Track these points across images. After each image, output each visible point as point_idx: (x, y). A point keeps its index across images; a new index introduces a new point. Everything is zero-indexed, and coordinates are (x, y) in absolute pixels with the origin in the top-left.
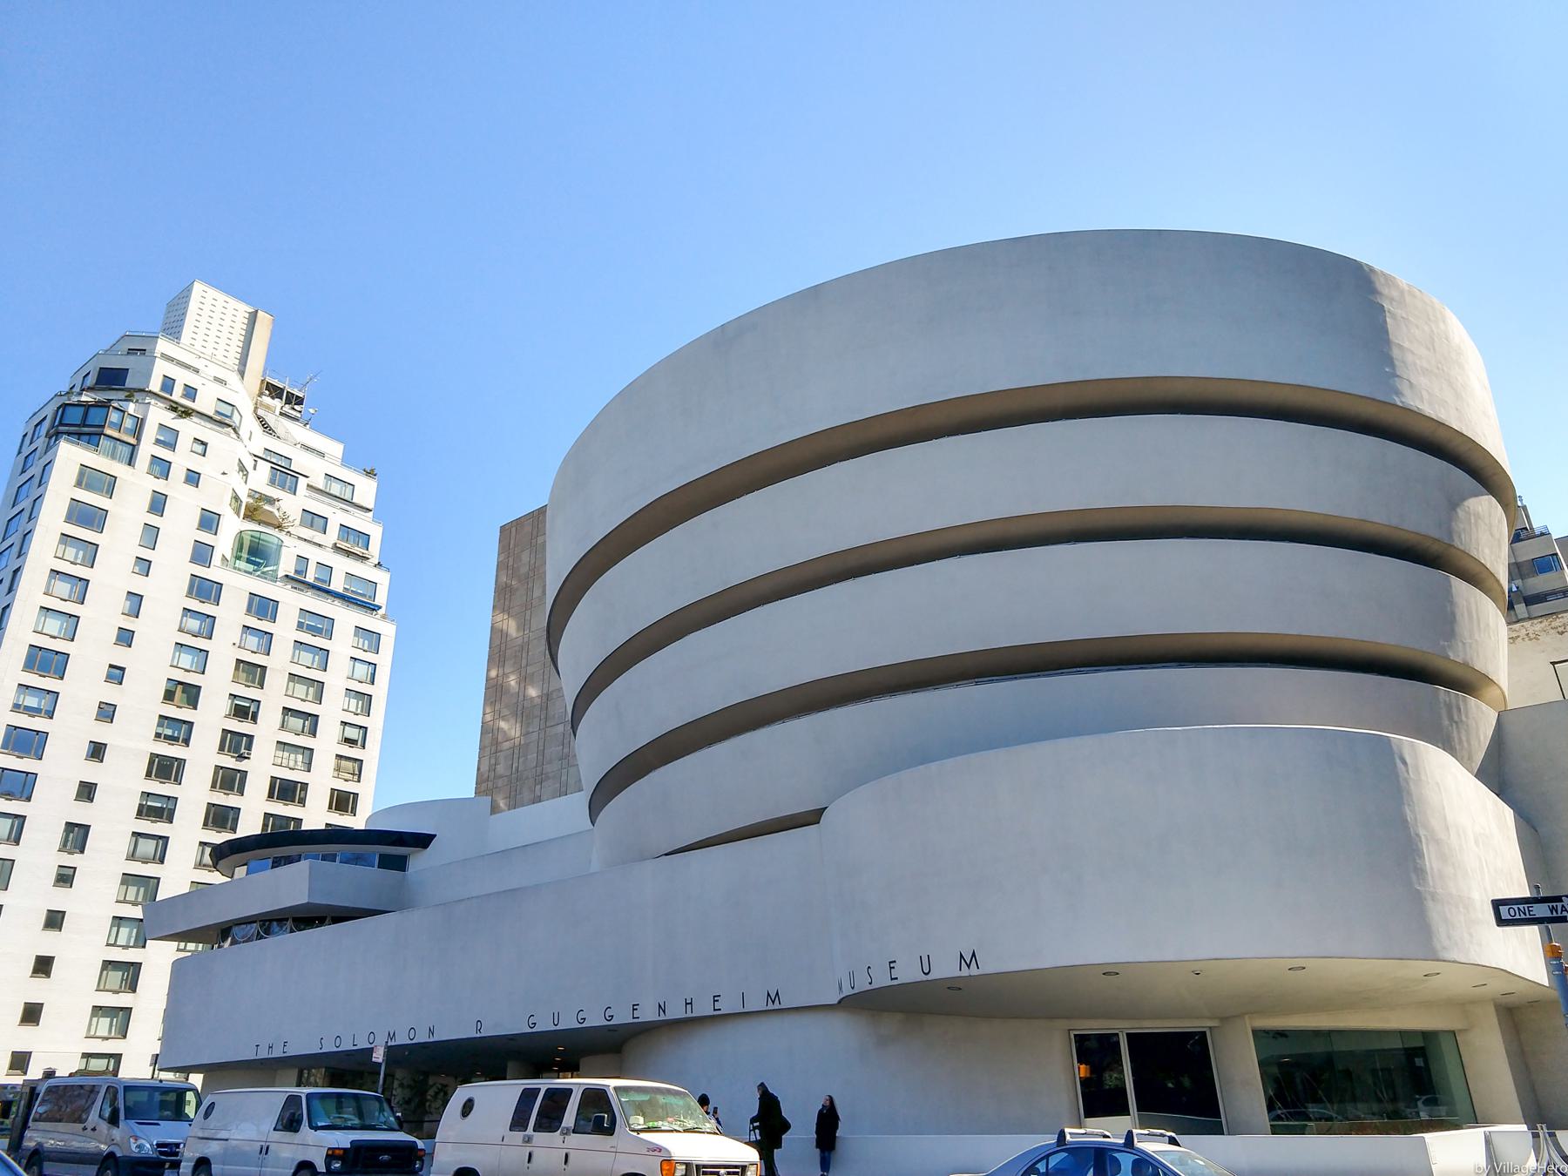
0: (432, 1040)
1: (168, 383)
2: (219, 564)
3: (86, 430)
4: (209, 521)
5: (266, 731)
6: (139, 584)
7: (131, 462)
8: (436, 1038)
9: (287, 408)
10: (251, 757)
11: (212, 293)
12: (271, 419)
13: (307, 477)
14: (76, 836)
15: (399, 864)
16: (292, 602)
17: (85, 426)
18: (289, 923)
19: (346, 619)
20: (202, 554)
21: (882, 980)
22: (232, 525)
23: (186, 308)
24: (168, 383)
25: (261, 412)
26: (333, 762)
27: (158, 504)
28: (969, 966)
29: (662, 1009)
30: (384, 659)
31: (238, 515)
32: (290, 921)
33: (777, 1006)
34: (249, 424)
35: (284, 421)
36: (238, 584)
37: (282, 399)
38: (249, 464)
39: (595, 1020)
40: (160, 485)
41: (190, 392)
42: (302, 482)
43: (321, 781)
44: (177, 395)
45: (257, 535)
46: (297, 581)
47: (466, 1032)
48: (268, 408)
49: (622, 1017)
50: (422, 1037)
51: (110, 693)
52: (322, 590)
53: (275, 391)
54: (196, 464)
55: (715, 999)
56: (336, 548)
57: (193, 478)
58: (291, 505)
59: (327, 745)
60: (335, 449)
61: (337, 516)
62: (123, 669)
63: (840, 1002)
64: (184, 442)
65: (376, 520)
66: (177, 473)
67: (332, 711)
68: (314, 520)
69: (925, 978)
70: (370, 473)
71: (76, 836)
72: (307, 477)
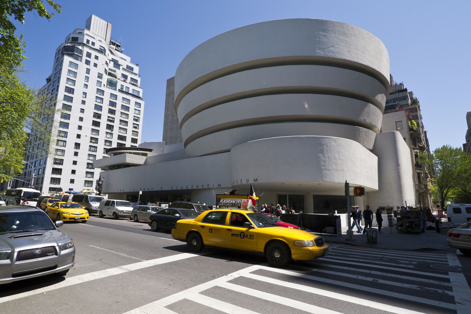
0: (152, 190)
1: (88, 41)
2: (103, 86)
4: (100, 76)
5: (116, 124)
6: (85, 90)
7: (81, 61)
8: (154, 190)
9: (117, 48)
10: (114, 130)
11: (97, 18)
12: (113, 51)
13: (122, 66)
14: (77, 145)
15: (146, 155)
16: (120, 95)
18: (123, 166)
19: (133, 100)
20: (99, 83)
21: (239, 183)
22: (106, 78)
23: (91, 22)
24: (88, 41)
26: (131, 132)
27: (88, 71)
28: (256, 181)
29: (198, 186)
30: (142, 109)
31: (107, 74)
32: (123, 166)
33: (220, 187)
34: (108, 52)
35: (116, 51)
36: (108, 91)
37: (115, 46)
38: (108, 62)
39: (184, 188)
40: (88, 67)
41: (93, 44)
42: (121, 67)
43: (129, 136)
44: (90, 44)
45: (111, 79)
46: (121, 91)
47: (160, 189)
48: (112, 48)
49: (190, 188)
50: (150, 190)
52: (127, 93)
53: (114, 44)
54: (96, 61)
55: (208, 185)
56: (130, 83)
57: (95, 65)
58: (119, 73)
59: (130, 128)
60: (128, 59)
61: (130, 76)
62: (84, 110)
63: (232, 187)
64: (93, 56)
65: (139, 76)
66: (92, 64)
67: (131, 121)
68: (125, 77)
69: (247, 183)
70: (137, 65)
71: (77, 145)
72: (122, 66)
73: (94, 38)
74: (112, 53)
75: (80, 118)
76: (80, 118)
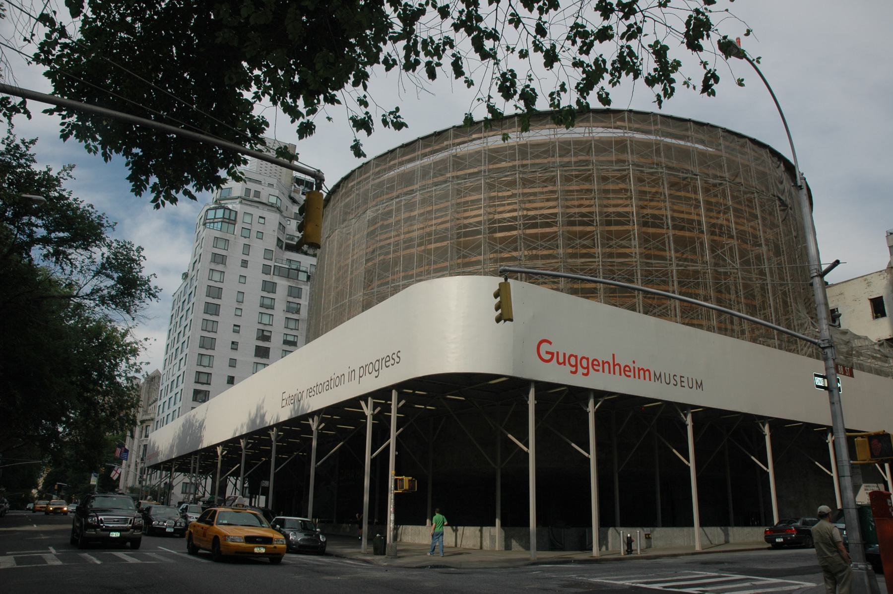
3: (216, 220)
17: (215, 218)
25: (293, 195)
27: (247, 247)
31: (282, 249)
40: (246, 241)
41: (257, 194)
51: (235, 338)
54: (260, 228)
57: (260, 235)
62: (239, 326)
64: (256, 218)
66: (254, 234)
73: (259, 182)
75: (233, 343)
76: (233, 343)
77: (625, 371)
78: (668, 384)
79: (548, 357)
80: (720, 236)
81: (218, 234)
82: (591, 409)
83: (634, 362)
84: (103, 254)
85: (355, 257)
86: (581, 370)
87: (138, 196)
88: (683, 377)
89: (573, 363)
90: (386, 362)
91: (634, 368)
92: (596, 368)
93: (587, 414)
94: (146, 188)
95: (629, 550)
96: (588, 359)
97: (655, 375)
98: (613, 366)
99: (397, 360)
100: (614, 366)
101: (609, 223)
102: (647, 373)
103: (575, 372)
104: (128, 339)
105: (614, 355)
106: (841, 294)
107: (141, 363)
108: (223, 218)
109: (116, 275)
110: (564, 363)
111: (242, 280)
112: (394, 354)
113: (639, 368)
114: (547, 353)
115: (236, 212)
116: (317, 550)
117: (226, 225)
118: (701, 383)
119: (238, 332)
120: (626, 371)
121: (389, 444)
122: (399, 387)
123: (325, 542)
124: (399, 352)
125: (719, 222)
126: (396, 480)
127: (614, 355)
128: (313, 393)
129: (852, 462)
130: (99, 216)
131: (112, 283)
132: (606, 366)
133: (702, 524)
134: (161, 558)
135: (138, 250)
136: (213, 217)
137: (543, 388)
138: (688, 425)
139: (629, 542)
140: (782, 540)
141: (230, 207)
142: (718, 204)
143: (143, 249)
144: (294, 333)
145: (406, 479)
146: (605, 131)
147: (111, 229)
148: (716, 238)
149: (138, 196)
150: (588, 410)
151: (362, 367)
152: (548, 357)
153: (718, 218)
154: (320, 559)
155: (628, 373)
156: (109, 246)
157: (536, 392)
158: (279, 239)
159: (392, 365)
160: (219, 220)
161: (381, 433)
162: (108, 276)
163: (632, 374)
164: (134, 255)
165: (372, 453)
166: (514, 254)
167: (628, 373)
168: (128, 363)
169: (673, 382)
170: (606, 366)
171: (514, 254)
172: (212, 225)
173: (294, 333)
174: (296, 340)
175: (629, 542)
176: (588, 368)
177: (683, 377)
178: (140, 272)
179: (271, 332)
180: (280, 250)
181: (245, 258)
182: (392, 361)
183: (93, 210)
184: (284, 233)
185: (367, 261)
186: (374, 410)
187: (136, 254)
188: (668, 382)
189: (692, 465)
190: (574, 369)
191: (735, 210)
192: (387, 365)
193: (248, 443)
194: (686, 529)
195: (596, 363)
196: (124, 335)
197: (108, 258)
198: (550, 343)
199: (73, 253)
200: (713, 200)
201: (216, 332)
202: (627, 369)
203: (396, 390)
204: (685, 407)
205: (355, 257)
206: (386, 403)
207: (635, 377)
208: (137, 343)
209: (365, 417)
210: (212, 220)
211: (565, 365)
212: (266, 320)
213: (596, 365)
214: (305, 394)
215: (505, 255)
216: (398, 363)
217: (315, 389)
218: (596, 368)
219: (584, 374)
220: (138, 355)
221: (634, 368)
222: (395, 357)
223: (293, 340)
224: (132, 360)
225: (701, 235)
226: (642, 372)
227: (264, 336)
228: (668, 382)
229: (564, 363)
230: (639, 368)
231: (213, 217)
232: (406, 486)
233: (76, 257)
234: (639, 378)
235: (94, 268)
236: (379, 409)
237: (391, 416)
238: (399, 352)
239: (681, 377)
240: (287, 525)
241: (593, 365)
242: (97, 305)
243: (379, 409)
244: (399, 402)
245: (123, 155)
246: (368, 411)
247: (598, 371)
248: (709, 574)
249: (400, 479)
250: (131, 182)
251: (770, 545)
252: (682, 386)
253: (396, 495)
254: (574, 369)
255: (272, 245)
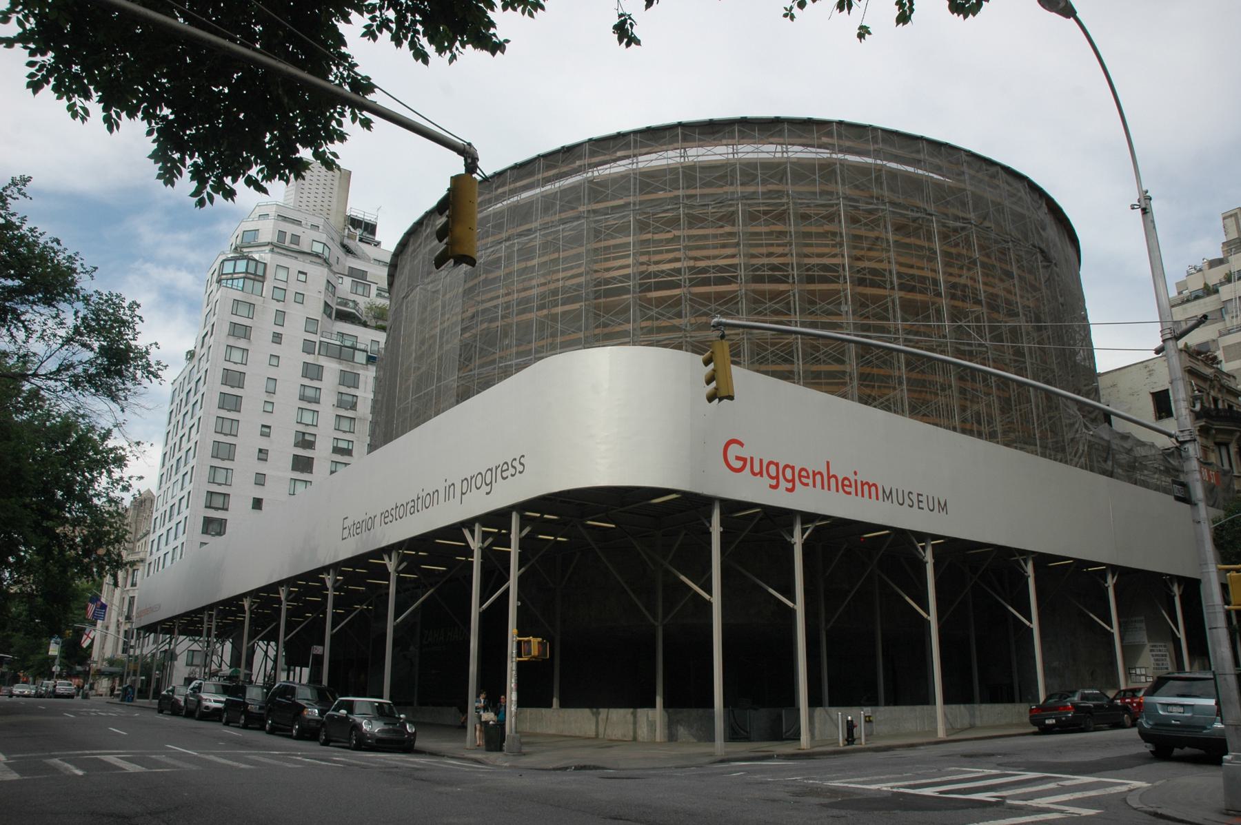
3: (235, 276)
6: (272, 373)
9: (365, 234)
12: (351, 244)
17: (234, 273)
25: (346, 241)
27: (281, 316)
35: (361, 244)
40: (280, 306)
41: (296, 239)
51: (264, 443)
57: (300, 298)
62: (269, 427)
66: (290, 296)
73: (298, 223)
74: (348, 250)
75: (260, 451)
76: (260, 451)
77: (843, 485)
78: (902, 504)
79: (738, 464)
80: (963, 301)
81: (239, 295)
82: (798, 539)
83: (855, 473)
84: (76, 313)
85: (446, 325)
86: (784, 484)
87: (169, 185)
88: (922, 495)
89: (773, 473)
90: (502, 471)
91: (856, 481)
92: (804, 480)
93: (791, 547)
94: (181, 173)
95: (850, 738)
96: (793, 468)
97: (884, 492)
98: (827, 479)
99: (520, 468)
100: (829, 478)
101: (810, 280)
102: (873, 489)
103: (775, 487)
104: (110, 443)
105: (828, 463)
106: (1114, 386)
107: (130, 478)
108: (247, 272)
109: (96, 345)
110: (761, 473)
111: (274, 362)
112: (515, 459)
113: (862, 482)
114: (738, 458)
115: (265, 264)
116: (403, 745)
117: (249, 283)
118: (945, 504)
119: (268, 436)
120: (844, 485)
121: (508, 589)
122: (522, 507)
123: (414, 734)
124: (523, 456)
125: (962, 281)
126: (519, 643)
127: (828, 463)
128: (390, 518)
129: (1226, 607)
130: (70, 257)
131: (91, 355)
132: (818, 478)
133: (947, 701)
134: (180, 764)
135: (130, 307)
136: (232, 271)
137: (731, 507)
138: (927, 562)
139: (850, 726)
140: (1054, 721)
141: (256, 256)
142: (959, 255)
143: (139, 306)
144: (348, 437)
145: (535, 642)
146: (806, 150)
147: (87, 276)
148: (959, 304)
149: (169, 185)
150: (793, 540)
151: (466, 479)
152: (738, 464)
153: (960, 276)
154: (412, 760)
155: (847, 489)
156: (86, 300)
157: (721, 514)
158: (326, 304)
159: (512, 475)
160: (241, 275)
161: (495, 573)
162: (84, 345)
163: (852, 490)
164: (124, 314)
165: (481, 604)
166: (676, 322)
167: (847, 489)
168: (110, 476)
169: (907, 501)
170: (818, 478)
171: (676, 322)
172: (230, 282)
173: (348, 437)
174: (350, 448)
175: (850, 726)
176: (793, 481)
177: (922, 495)
178: (134, 339)
179: (315, 435)
180: (329, 319)
181: (278, 330)
182: (512, 471)
183: (59, 247)
184: (334, 296)
185: (464, 330)
186: (483, 543)
187: (128, 312)
188: (901, 502)
189: (933, 618)
190: (774, 482)
191: (984, 265)
192: (505, 474)
193: (290, 593)
194: (918, 709)
195: (804, 473)
196: (107, 435)
197: (85, 318)
198: (742, 444)
199: (27, 312)
200: (953, 251)
201: (236, 436)
202: (846, 482)
203: (517, 512)
204: (922, 537)
205: (446, 325)
206: (499, 534)
207: (857, 495)
208: (124, 450)
209: (470, 553)
210: (229, 276)
211: (762, 476)
212: (308, 418)
213: (805, 477)
214: (377, 520)
215: (664, 323)
216: (520, 472)
217: (393, 512)
218: (804, 480)
219: (788, 490)
220: (126, 465)
221: (856, 481)
222: (516, 464)
223: (346, 447)
224: (117, 474)
225: (937, 299)
226: (866, 487)
227: (305, 441)
228: (901, 502)
229: (761, 473)
230: (862, 482)
231: (232, 271)
232: (535, 651)
233: (33, 317)
234: (863, 496)
235: (62, 333)
236: (490, 540)
237: (510, 552)
238: (523, 456)
239: (919, 495)
240: (357, 710)
241: (800, 476)
242: (66, 389)
243: (490, 540)
244: (521, 531)
245: (143, 119)
246: (475, 544)
247: (807, 485)
248: (988, 772)
249: (525, 642)
250: (156, 162)
251: (1036, 729)
252: (919, 508)
253: (519, 664)
254: (774, 482)
255: (317, 312)
